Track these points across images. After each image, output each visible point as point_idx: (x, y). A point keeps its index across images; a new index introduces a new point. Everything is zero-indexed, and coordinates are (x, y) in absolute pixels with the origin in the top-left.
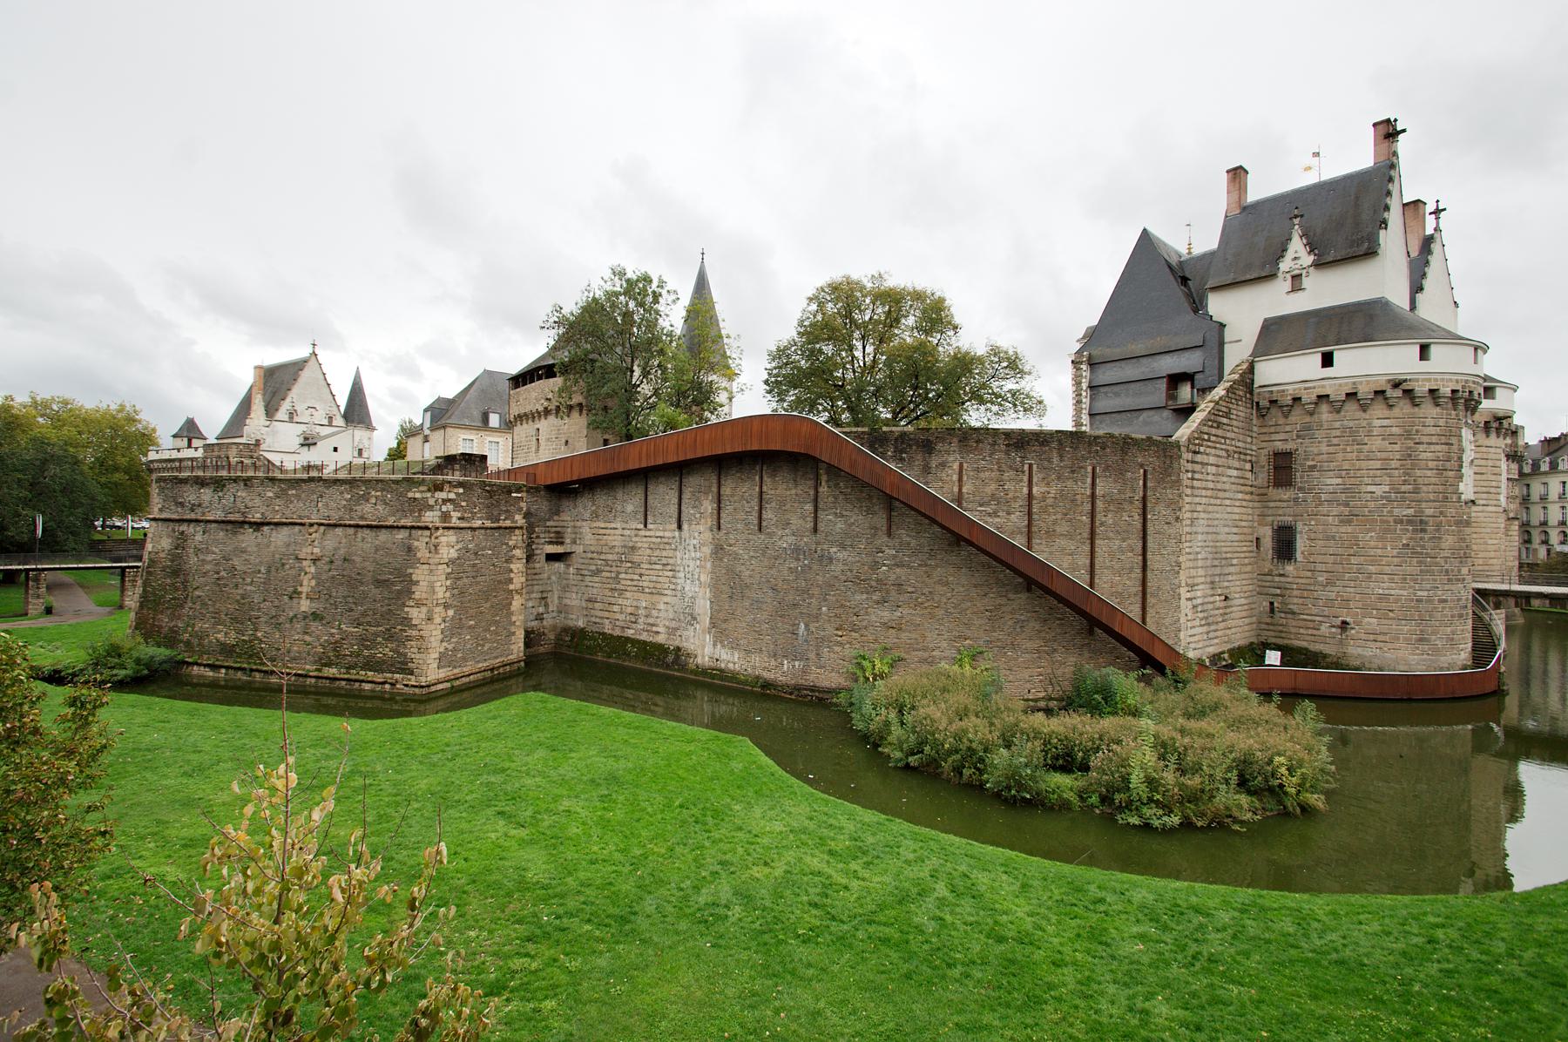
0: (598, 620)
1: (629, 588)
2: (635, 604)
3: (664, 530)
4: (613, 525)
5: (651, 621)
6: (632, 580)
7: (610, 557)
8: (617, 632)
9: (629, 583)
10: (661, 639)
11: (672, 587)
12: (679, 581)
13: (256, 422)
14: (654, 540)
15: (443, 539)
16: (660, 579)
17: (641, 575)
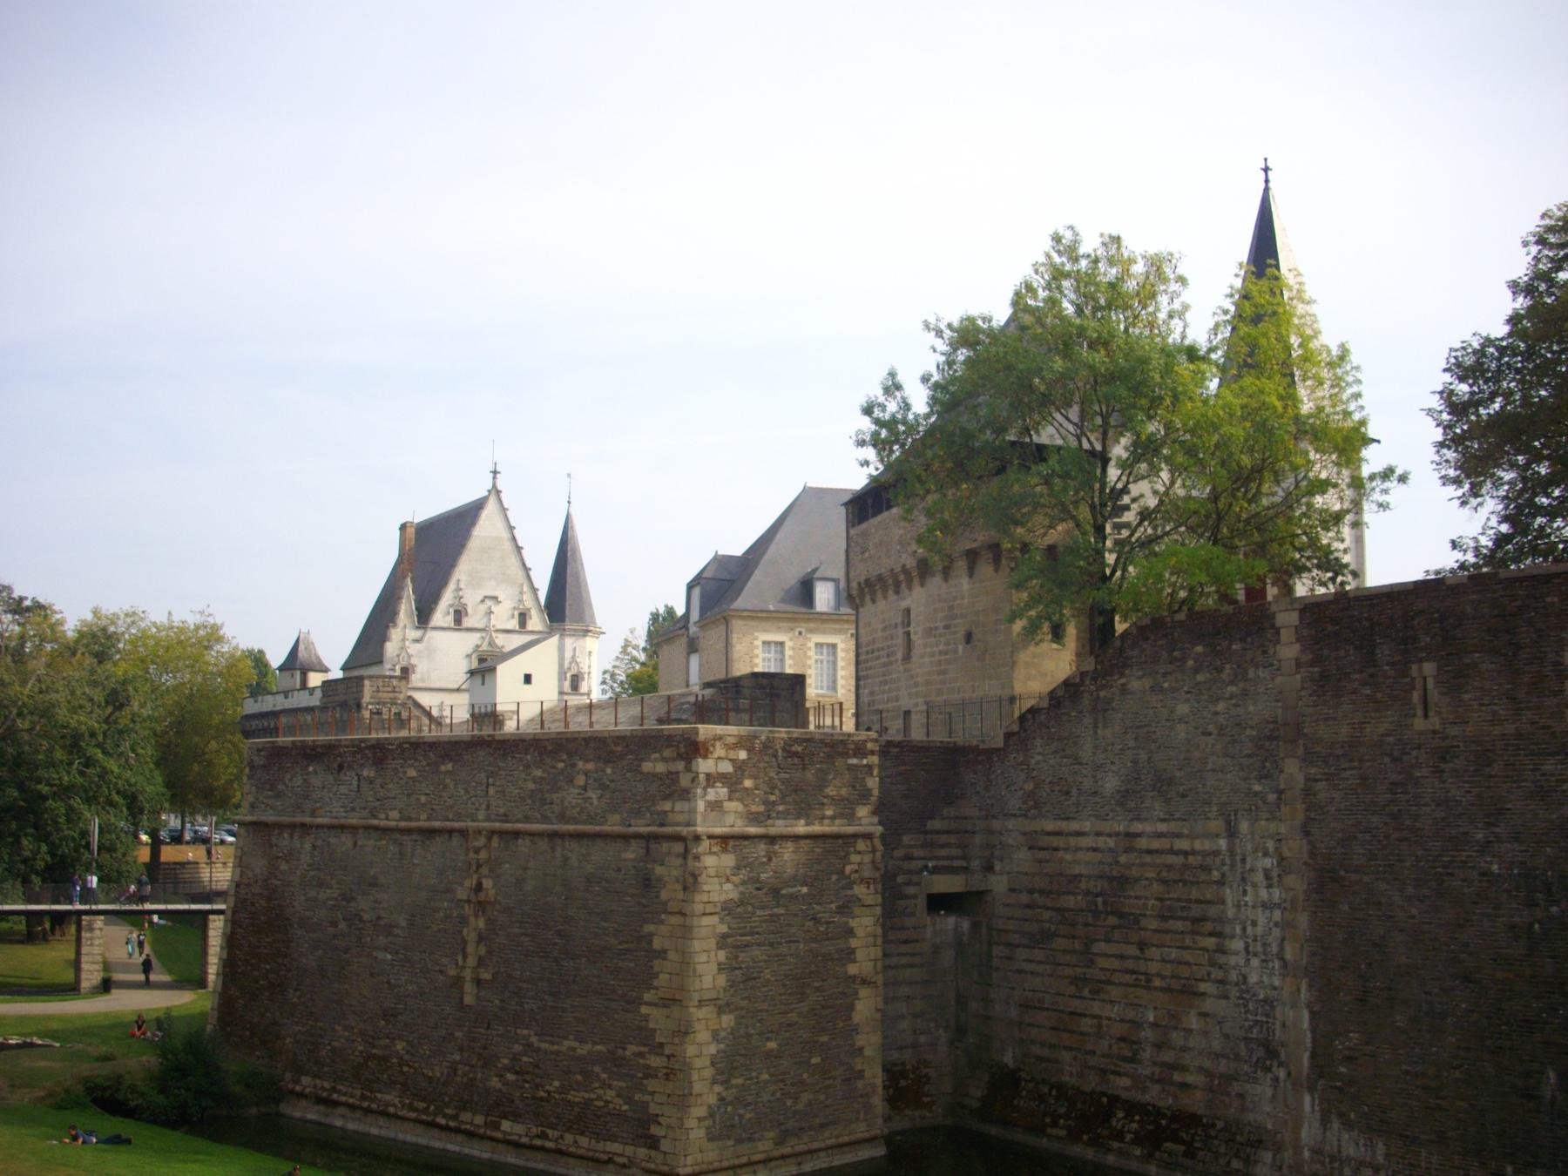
0: (1046, 1052)
1: (1116, 977)
2: (1130, 1014)
3: (1192, 836)
4: (1074, 826)
5: (1168, 1056)
6: (1122, 957)
7: (1070, 902)
8: (1091, 1084)
9: (1116, 964)
10: (1196, 1102)
11: (1219, 974)
12: (1233, 960)
13: (401, 638)
14: (1171, 859)
15: (709, 861)
16: (1187, 956)
17: (1142, 946)
